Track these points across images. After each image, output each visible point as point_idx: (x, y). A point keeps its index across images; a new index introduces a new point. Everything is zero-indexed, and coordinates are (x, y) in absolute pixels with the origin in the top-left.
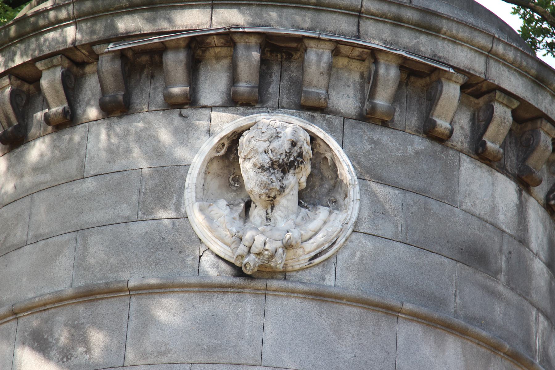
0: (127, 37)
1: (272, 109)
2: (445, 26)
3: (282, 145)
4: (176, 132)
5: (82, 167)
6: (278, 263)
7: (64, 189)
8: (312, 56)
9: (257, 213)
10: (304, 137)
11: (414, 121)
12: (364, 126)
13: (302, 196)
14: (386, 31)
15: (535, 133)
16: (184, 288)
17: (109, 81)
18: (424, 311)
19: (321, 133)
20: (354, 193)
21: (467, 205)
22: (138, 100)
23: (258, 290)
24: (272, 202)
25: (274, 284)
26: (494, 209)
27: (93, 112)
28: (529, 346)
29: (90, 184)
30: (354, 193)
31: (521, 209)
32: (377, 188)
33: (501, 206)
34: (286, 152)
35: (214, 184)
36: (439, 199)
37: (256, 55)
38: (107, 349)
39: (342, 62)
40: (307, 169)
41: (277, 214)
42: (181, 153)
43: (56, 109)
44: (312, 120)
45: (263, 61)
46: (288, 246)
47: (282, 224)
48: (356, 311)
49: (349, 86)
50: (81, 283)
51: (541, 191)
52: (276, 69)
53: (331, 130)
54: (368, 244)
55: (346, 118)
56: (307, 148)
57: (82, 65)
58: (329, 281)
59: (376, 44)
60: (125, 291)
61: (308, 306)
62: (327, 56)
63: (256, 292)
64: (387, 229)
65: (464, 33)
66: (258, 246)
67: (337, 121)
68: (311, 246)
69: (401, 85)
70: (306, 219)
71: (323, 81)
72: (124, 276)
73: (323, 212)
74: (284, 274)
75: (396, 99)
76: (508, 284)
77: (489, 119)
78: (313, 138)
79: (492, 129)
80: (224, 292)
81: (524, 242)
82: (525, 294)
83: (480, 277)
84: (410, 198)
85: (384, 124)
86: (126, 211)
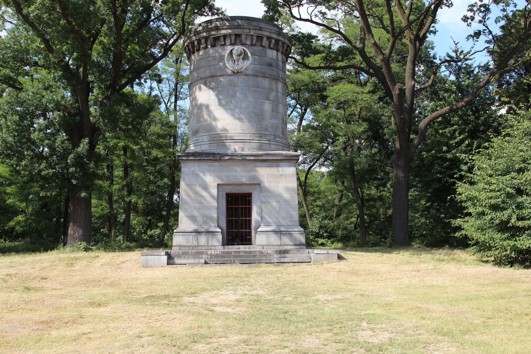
0: (214, 35)
1: (237, 45)
2: (263, 29)
3: (239, 52)
4: (222, 50)
5: (209, 55)
6: (240, 71)
7: (207, 59)
8: (243, 36)
9: (236, 62)
10: (242, 50)
11: (259, 44)
12: (252, 46)
13: (243, 58)
14: (254, 31)
15: (279, 43)
16: (226, 75)
17: (212, 42)
18: (262, 75)
19: (244, 48)
20: (251, 58)
21: (268, 57)
22: (217, 44)
24: (238, 61)
25: (239, 74)
26: (273, 56)
27: (209, 47)
28: (279, 77)
29: (210, 58)
30: (251, 58)
31: (277, 55)
33: (274, 55)
35: (229, 57)
36: (264, 57)
37: (234, 37)
38: (215, 85)
39: (248, 36)
40: (243, 55)
41: (239, 62)
42: (223, 53)
43: (204, 46)
44: (243, 46)
45: (235, 37)
46: (241, 68)
47: (240, 64)
48: (252, 77)
50: (210, 75)
51: (280, 51)
52: (237, 38)
53: (246, 48)
54: (253, 66)
55: (249, 45)
56: (243, 52)
57: (207, 38)
58: (248, 72)
59: (252, 34)
61: (245, 77)
62: (245, 36)
63: (237, 75)
64: (256, 63)
65: (266, 30)
66: (236, 69)
67: (247, 46)
68: (244, 67)
69: (257, 38)
70: (244, 63)
71: (245, 40)
72: (216, 73)
73: (246, 61)
74: (241, 72)
75: (256, 41)
76: (275, 68)
77: (271, 42)
78: (244, 49)
79: (272, 44)
81: (278, 60)
82: (278, 69)
83: (271, 68)
84: (259, 57)
85: (255, 46)
86: (216, 63)
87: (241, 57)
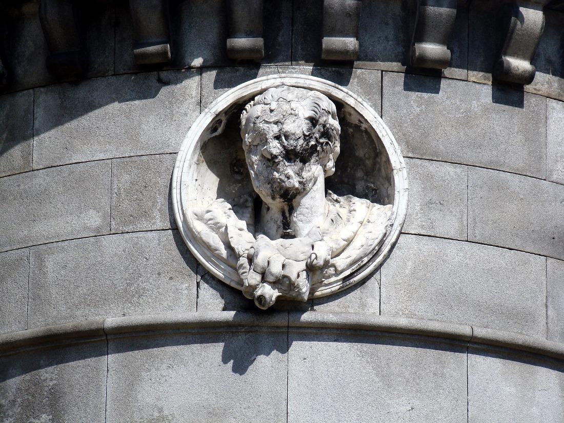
3: (297, 127)
23: (278, 327)
30: (401, 180)
32: (432, 167)
34: (304, 135)
49: (387, 24)
56: (335, 123)
60: (101, 336)
64: (449, 225)
80: (232, 332)
87: (316, 171)
